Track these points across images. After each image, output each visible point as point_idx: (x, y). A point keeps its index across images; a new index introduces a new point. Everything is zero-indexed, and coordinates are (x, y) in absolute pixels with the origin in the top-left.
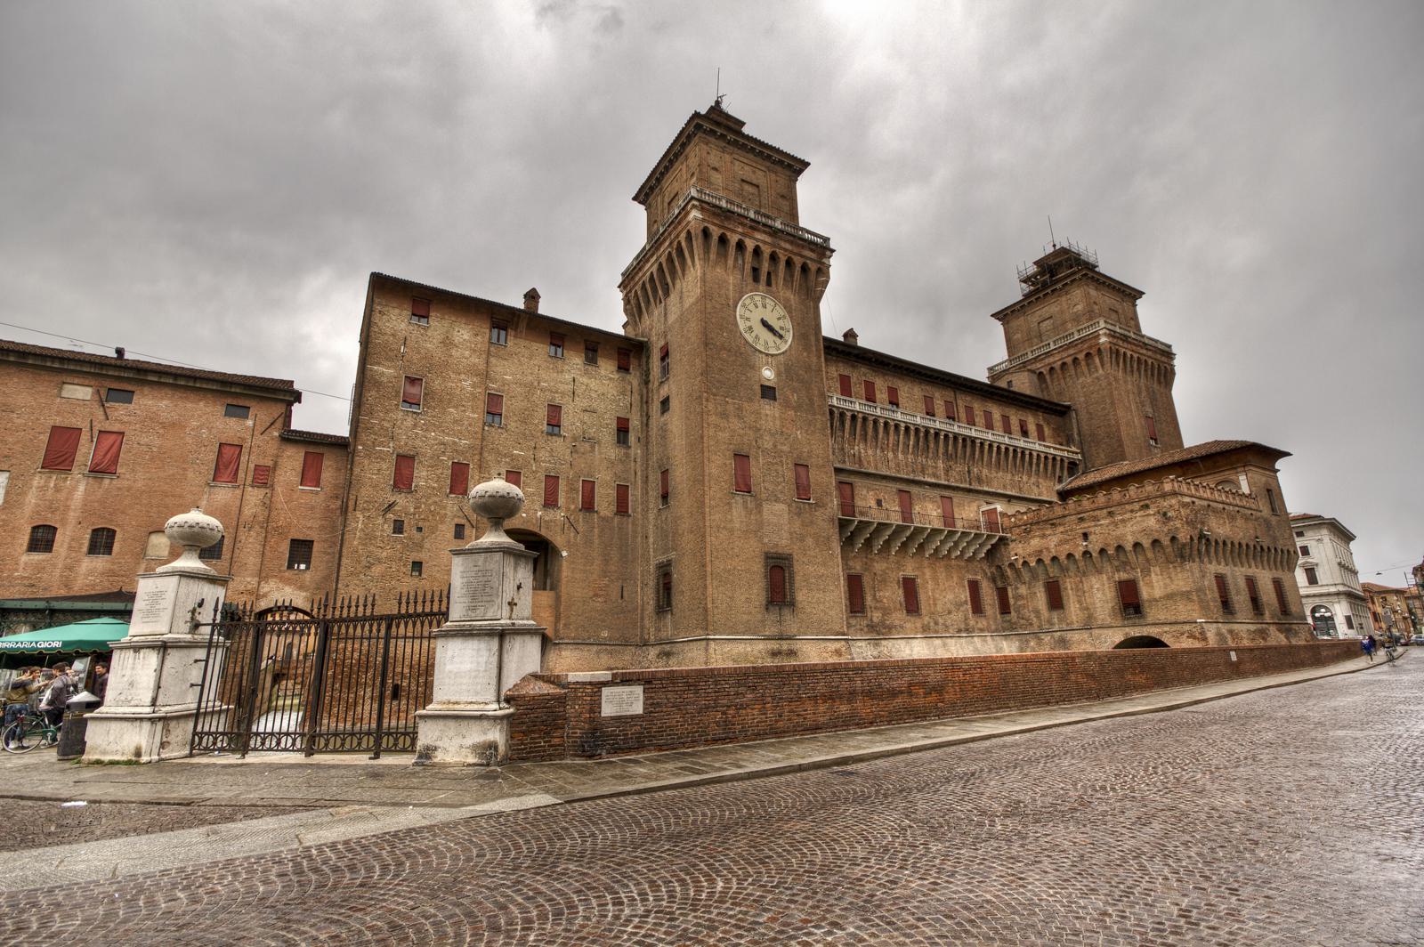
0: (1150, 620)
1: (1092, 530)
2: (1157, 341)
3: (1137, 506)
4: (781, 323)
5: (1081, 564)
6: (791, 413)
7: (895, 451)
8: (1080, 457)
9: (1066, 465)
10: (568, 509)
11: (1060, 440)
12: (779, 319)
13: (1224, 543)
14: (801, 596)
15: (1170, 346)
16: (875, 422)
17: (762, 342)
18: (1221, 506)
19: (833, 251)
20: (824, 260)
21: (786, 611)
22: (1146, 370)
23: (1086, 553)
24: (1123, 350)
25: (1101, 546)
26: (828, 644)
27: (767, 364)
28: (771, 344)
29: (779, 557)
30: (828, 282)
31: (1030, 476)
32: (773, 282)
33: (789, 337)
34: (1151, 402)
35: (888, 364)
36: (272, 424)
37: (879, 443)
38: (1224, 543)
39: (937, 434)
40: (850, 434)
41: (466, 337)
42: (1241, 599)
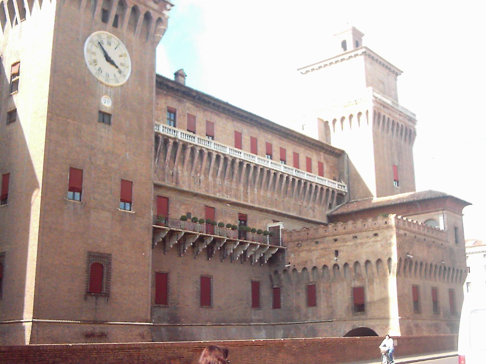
0: (369, 316)
1: (341, 248)
2: (407, 110)
3: (371, 234)
4: (122, 60)
5: (331, 273)
6: (123, 137)
7: (206, 174)
8: (345, 190)
9: (336, 195)
11: (334, 175)
12: (121, 56)
13: (421, 264)
14: (116, 289)
15: (415, 115)
16: (193, 149)
17: (104, 74)
18: (423, 237)
19: (172, 5)
20: (165, 12)
21: (102, 300)
22: (397, 130)
23: (336, 265)
24: (382, 114)
25: (346, 261)
27: (106, 93)
28: (111, 77)
30: (165, 30)
31: (308, 201)
32: (119, 24)
33: (128, 73)
34: (398, 155)
35: (209, 103)
37: (194, 167)
38: (421, 264)
39: (241, 163)
40: (171, 157)
42: (426, 302)
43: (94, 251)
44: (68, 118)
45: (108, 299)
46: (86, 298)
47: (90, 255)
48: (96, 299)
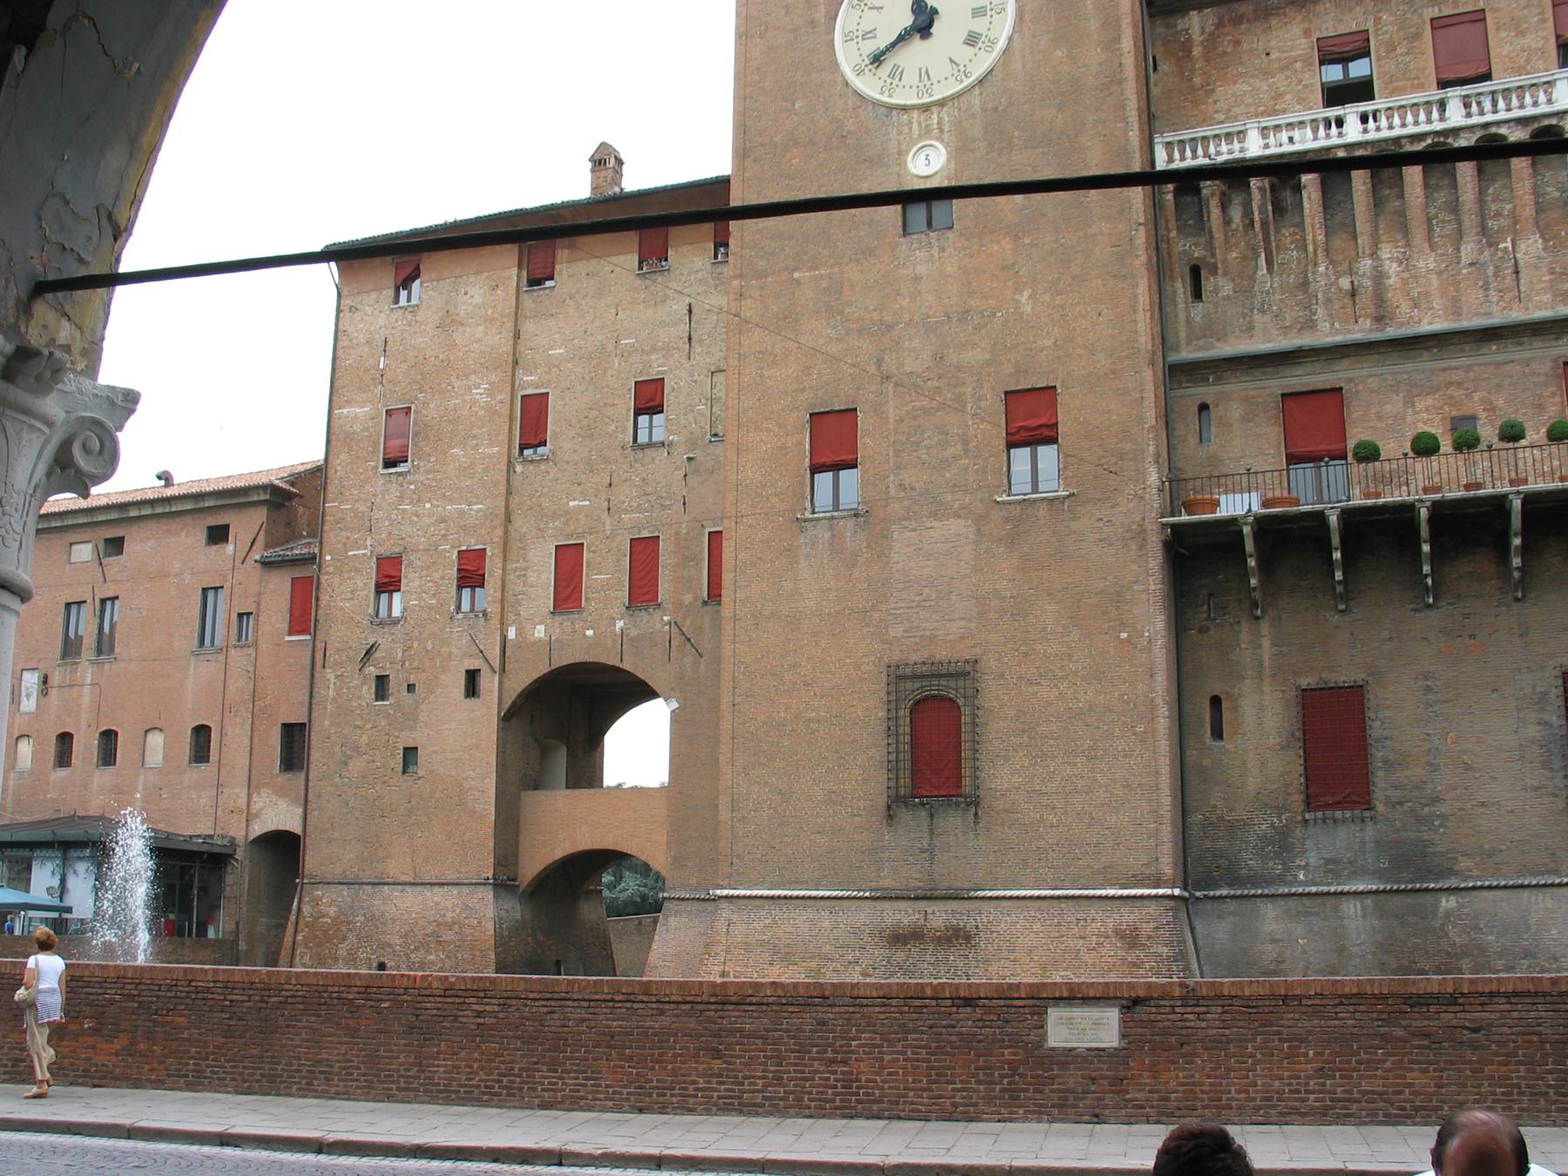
10: (678, 605)
21: (952, 821)
26: (1094, 911)
27: (926, 132)
29: (937, 672)
36: (252, 544)
41: (478, 299)
43: (915, 657)
44: (796, 269)
45: (976, 814)
46: (890, 817)
47: (898, 676)
48: (932, 816)
